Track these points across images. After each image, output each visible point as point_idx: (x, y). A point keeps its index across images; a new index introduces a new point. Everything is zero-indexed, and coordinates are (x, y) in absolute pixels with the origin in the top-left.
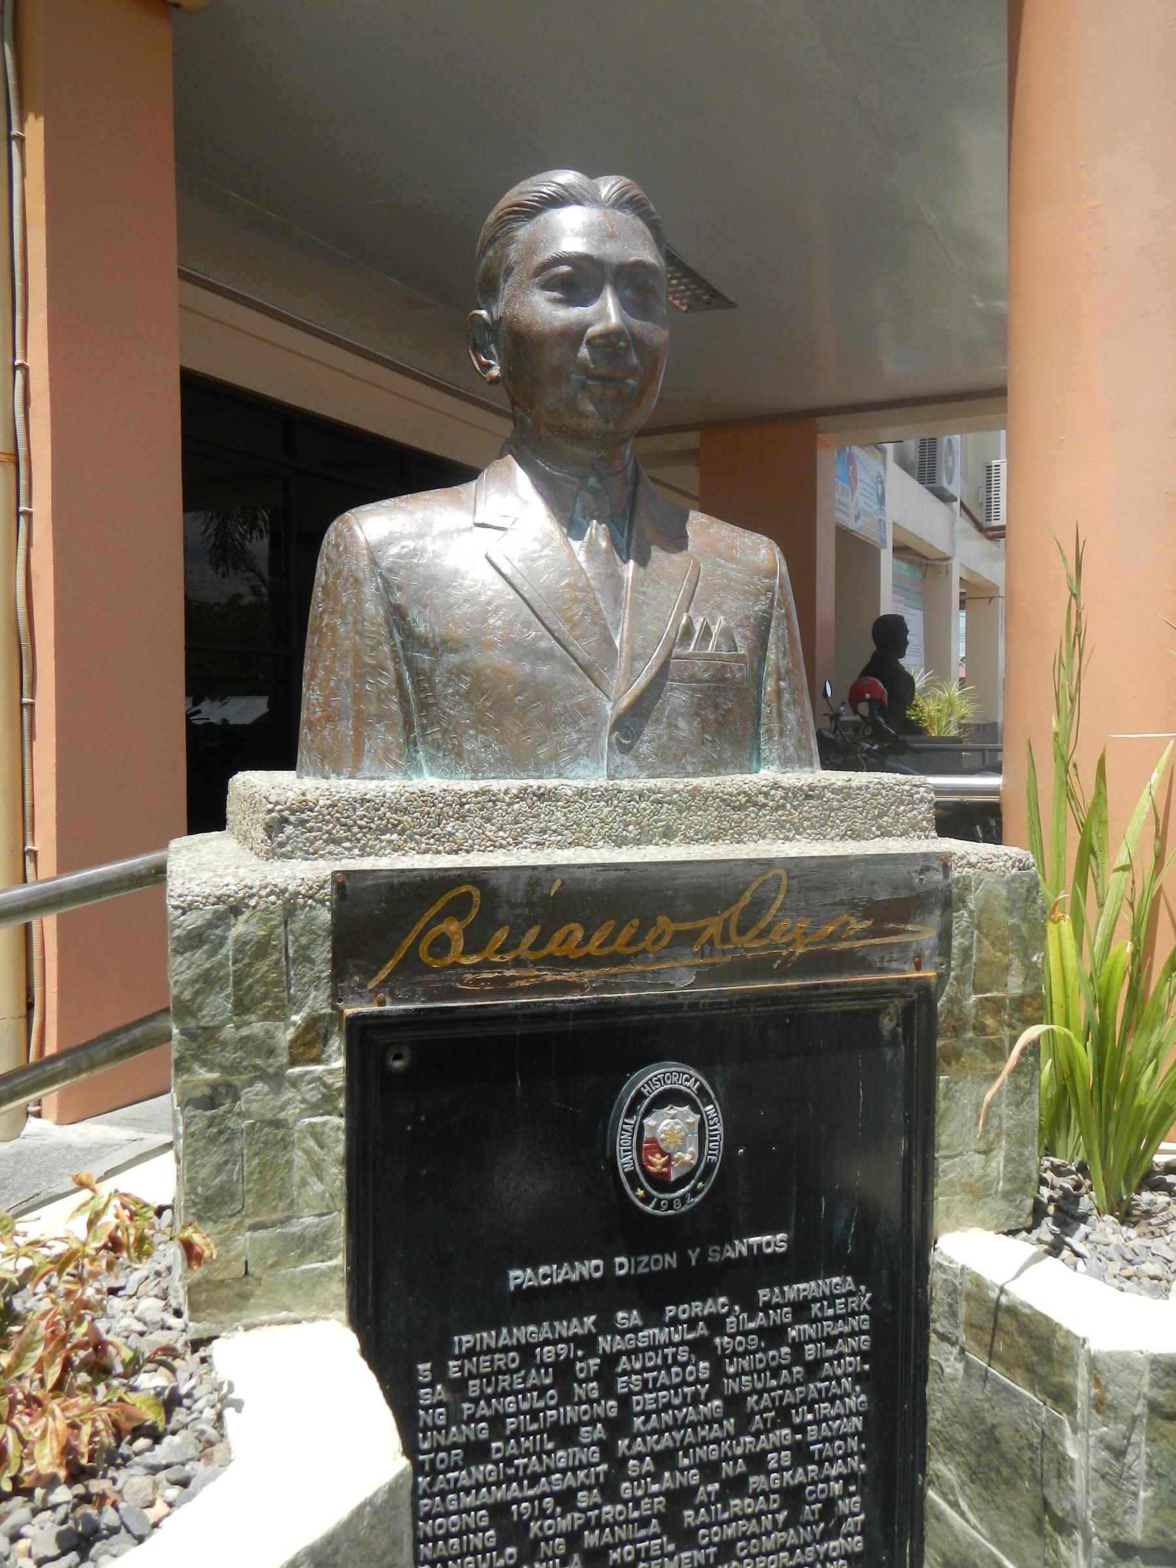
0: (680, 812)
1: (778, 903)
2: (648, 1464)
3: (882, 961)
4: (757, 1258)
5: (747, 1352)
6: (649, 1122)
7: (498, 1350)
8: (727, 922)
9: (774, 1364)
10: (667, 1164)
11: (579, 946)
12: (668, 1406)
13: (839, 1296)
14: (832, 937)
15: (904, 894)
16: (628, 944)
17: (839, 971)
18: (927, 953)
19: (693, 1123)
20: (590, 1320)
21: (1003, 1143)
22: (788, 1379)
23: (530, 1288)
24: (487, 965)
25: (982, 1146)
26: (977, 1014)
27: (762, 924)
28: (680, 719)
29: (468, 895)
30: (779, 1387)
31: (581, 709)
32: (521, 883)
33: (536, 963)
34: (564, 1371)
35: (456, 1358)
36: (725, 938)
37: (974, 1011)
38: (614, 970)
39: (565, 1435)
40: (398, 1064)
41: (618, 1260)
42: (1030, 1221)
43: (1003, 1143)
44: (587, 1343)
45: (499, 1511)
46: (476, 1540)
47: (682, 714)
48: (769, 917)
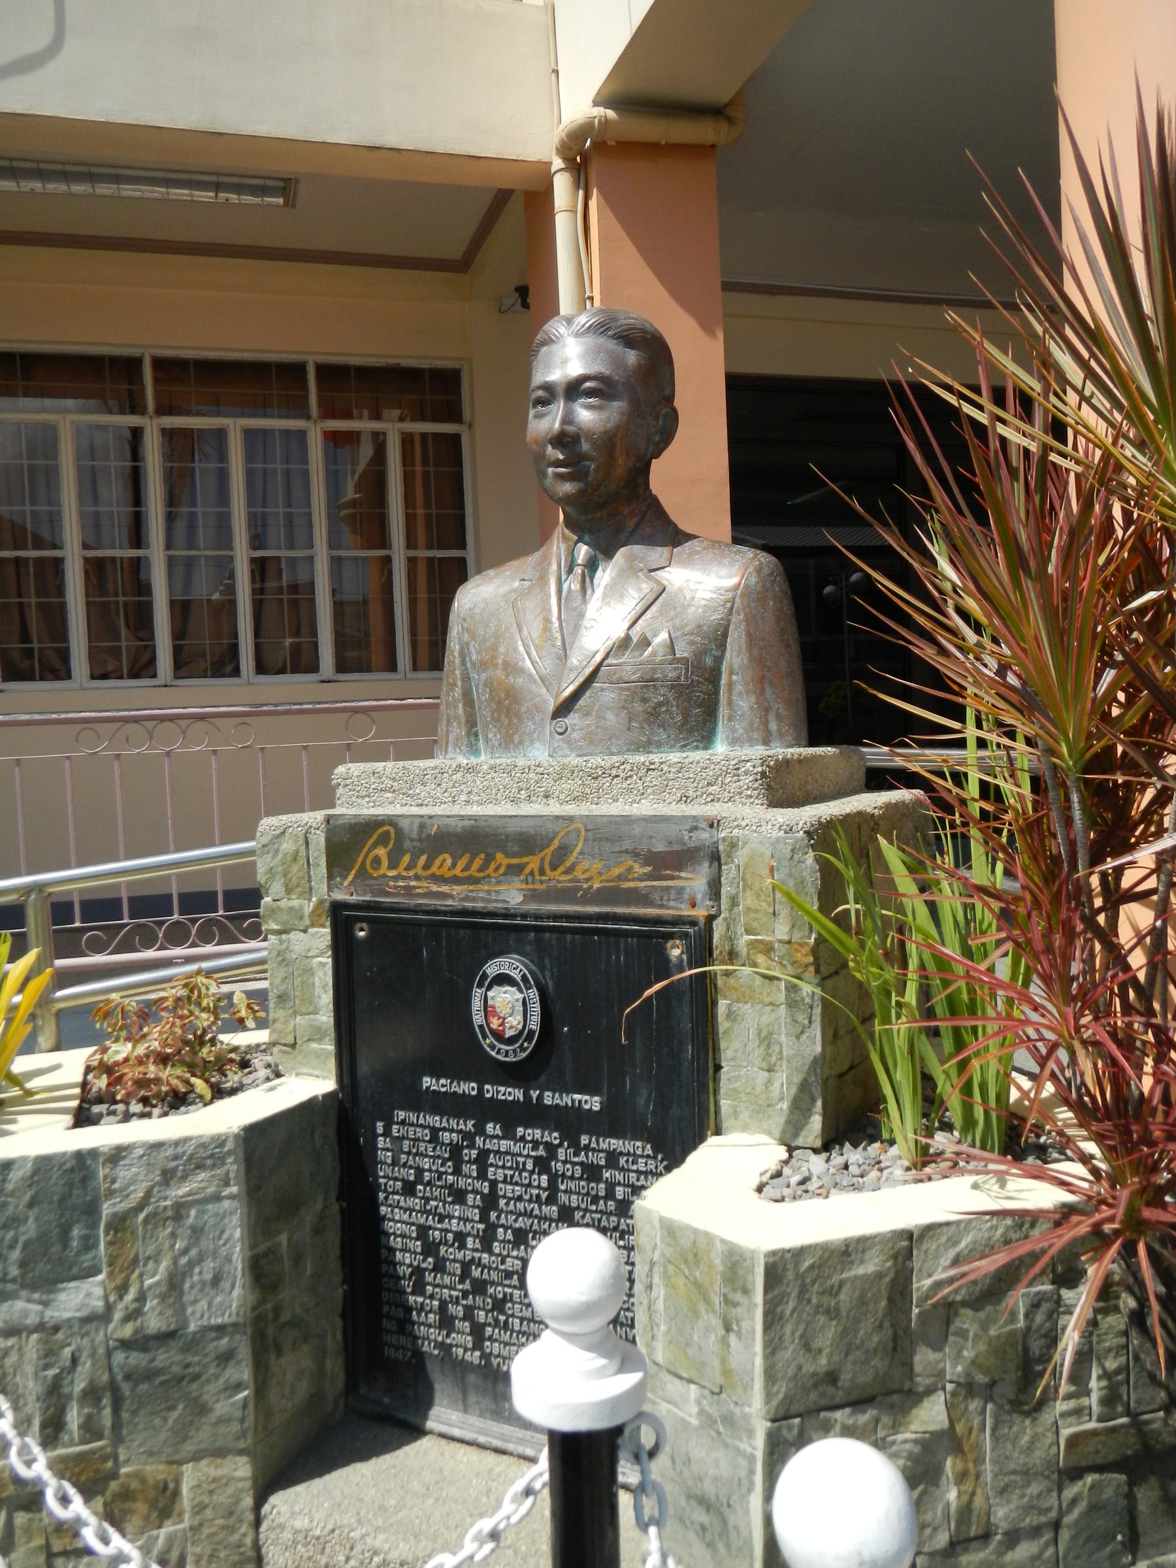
0: (555, 781)
1: (578, 849)
2: (510, 1236)
3: (662, 899)
4: (577, 1110)
5: (572, 1178)
6: (490, 994)
7: (417, 1126)
8: (542, 860)
9: (594, 1193)
10: (502, 1024)
11: (449, 869)
12: (520, 1198)
13: (642, 1156)
14: (620, 878)
15: (676, 848)
16: (479, 871)
17: (628, 903)
18: (699, 897)
19: (517, 1000)
20: (470, 1124)
21: (784, 1067)
22: (603, 1208)
23: (434, 1091)
24: (398, 877)
25: (764, 1065)
26: (748, 954)
27: (568, 864)
28: (608, 712)
29: (388, 832)
30: (596, 1212)
31: (537, 708)
32: (416, 827)
33: (426, 878)
34: (456, 1152)
35: (397, 1123)
36: (542, 872)
37: (745, 949)
38: (471, 888)
39: (459, 1196)
40: (362, 934)
41: (487, 1087)
42: (818, 1144)
43: (784, 1067)
44: (469, 1137)
45: (423, 1231)
46: (411, 1245)
47: (610, 709)
48: (572, 858)
